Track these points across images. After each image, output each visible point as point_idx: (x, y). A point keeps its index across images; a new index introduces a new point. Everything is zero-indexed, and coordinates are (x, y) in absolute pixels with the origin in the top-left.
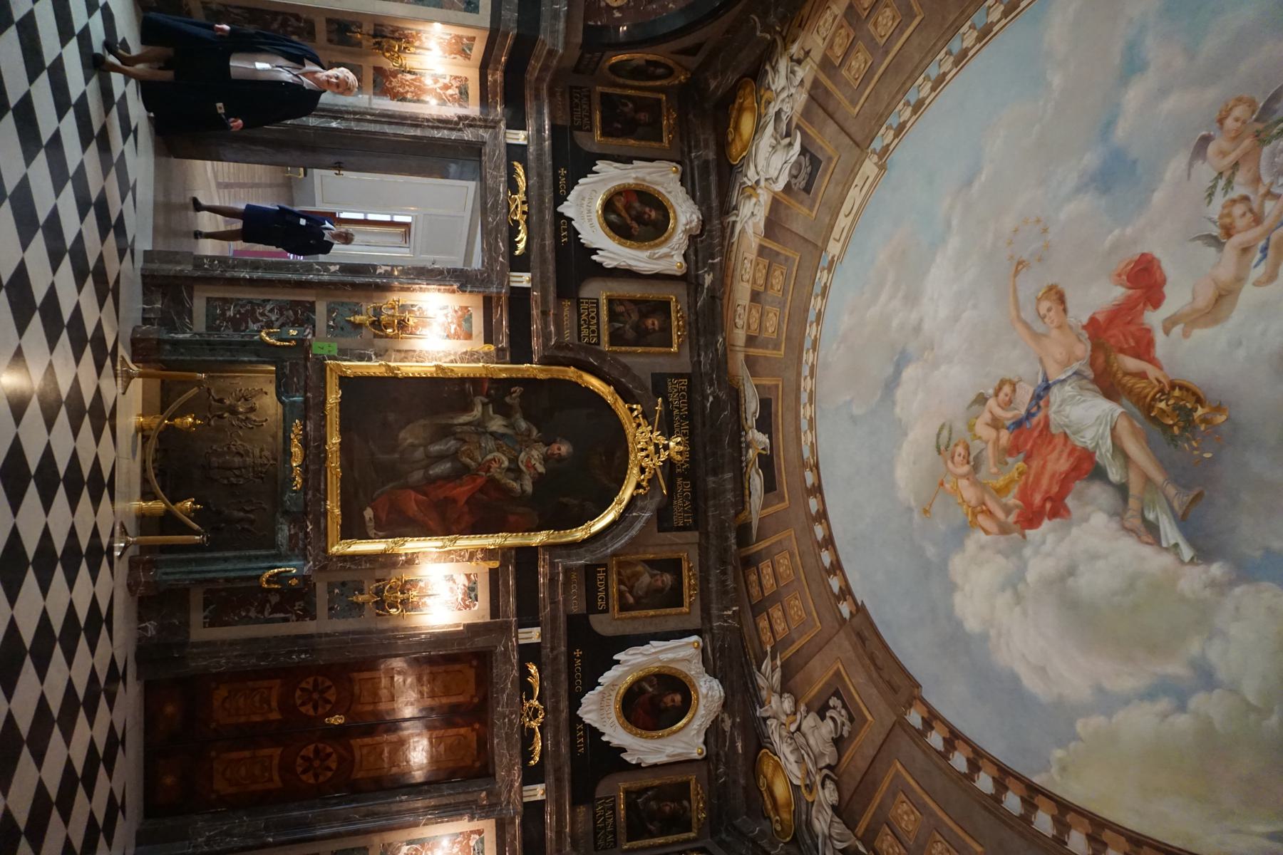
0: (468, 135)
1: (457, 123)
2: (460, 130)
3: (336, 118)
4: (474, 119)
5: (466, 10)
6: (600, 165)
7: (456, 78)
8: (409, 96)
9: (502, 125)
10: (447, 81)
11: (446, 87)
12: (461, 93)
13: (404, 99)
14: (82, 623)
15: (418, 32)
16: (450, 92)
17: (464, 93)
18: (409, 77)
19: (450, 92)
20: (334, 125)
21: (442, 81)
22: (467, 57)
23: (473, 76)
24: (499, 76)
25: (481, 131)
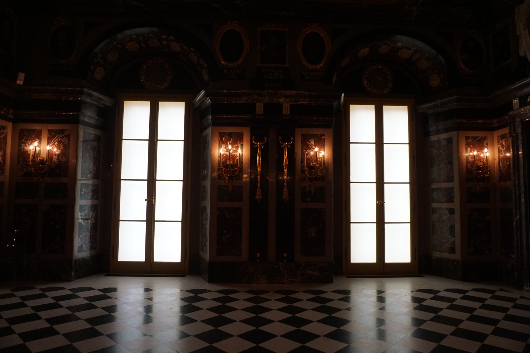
0: (519, 130)
1: (513, 137)
2: (517, 135)
3: (520, 199)
4: (510, 129)
5: (452, 143)
6: (522, 54)
7: (498, 142)
8: (508, 164)
9: (511, 113)
10: (500, 146)
11: (502, 146)
12: (503, 138)
13: (510, 165)
14: (222, 315)
15: (468, 162)
16: (504, 143)
17: (503, 137)
18: (501, 164)
19: (504, 143)
20: (523, 200)
21: (500, 148)
22: (485, 138)
23: (497, 133)
24: (494, 121)
25: (517, 124)
